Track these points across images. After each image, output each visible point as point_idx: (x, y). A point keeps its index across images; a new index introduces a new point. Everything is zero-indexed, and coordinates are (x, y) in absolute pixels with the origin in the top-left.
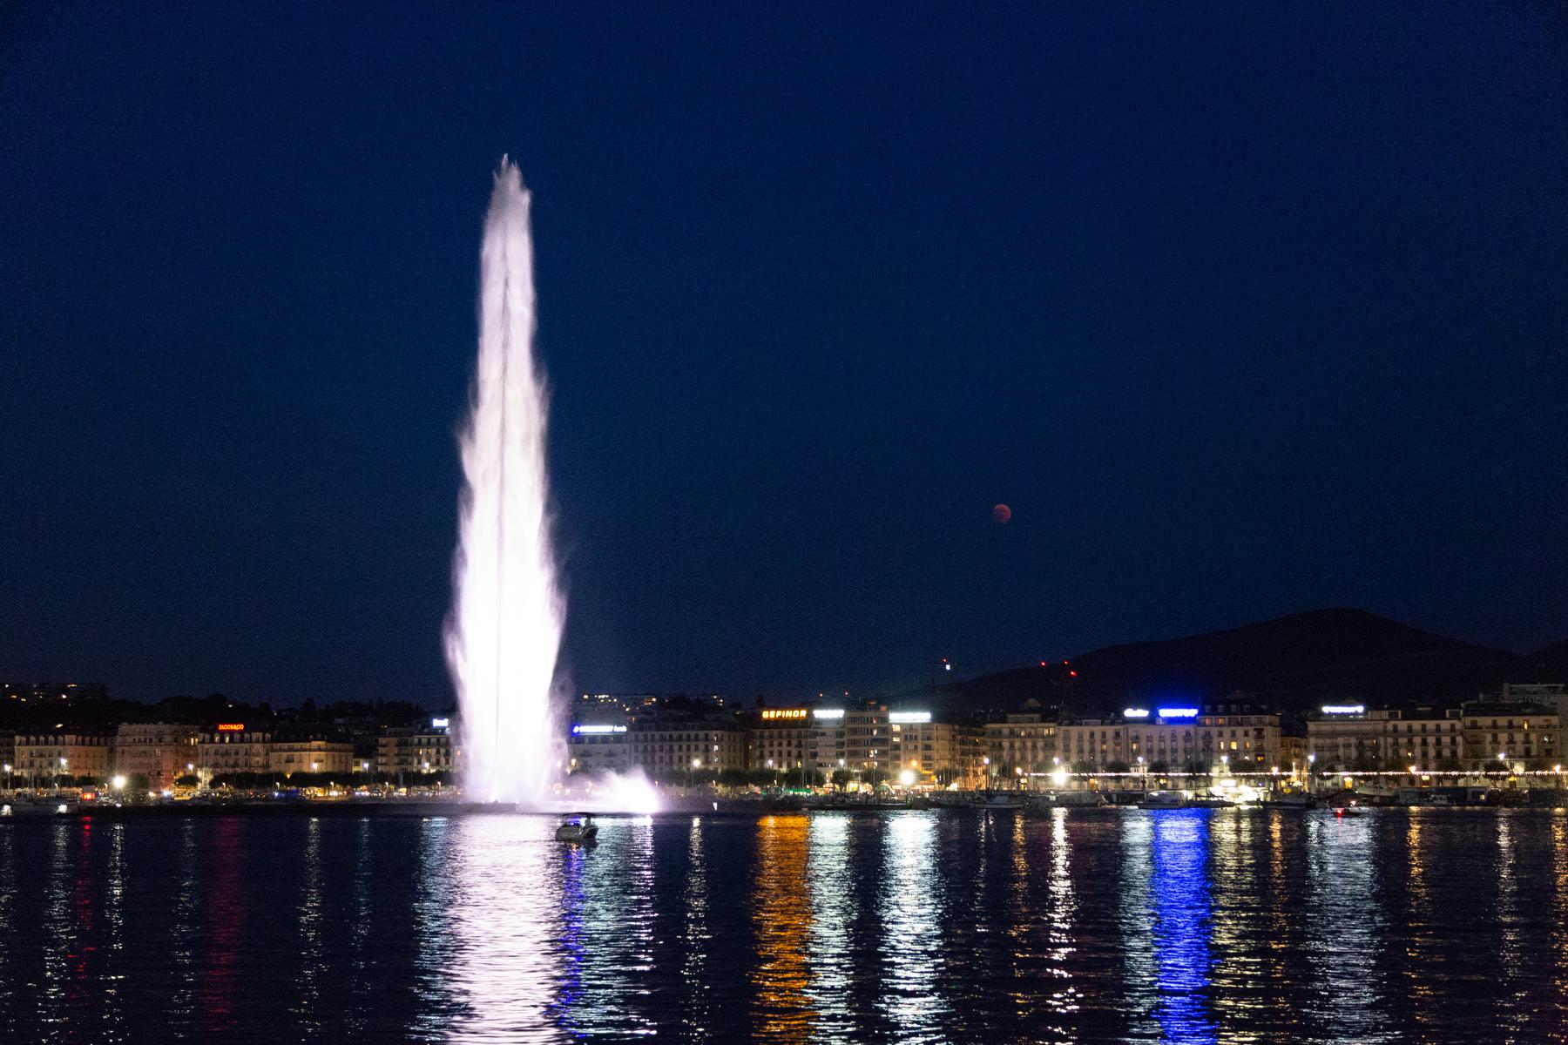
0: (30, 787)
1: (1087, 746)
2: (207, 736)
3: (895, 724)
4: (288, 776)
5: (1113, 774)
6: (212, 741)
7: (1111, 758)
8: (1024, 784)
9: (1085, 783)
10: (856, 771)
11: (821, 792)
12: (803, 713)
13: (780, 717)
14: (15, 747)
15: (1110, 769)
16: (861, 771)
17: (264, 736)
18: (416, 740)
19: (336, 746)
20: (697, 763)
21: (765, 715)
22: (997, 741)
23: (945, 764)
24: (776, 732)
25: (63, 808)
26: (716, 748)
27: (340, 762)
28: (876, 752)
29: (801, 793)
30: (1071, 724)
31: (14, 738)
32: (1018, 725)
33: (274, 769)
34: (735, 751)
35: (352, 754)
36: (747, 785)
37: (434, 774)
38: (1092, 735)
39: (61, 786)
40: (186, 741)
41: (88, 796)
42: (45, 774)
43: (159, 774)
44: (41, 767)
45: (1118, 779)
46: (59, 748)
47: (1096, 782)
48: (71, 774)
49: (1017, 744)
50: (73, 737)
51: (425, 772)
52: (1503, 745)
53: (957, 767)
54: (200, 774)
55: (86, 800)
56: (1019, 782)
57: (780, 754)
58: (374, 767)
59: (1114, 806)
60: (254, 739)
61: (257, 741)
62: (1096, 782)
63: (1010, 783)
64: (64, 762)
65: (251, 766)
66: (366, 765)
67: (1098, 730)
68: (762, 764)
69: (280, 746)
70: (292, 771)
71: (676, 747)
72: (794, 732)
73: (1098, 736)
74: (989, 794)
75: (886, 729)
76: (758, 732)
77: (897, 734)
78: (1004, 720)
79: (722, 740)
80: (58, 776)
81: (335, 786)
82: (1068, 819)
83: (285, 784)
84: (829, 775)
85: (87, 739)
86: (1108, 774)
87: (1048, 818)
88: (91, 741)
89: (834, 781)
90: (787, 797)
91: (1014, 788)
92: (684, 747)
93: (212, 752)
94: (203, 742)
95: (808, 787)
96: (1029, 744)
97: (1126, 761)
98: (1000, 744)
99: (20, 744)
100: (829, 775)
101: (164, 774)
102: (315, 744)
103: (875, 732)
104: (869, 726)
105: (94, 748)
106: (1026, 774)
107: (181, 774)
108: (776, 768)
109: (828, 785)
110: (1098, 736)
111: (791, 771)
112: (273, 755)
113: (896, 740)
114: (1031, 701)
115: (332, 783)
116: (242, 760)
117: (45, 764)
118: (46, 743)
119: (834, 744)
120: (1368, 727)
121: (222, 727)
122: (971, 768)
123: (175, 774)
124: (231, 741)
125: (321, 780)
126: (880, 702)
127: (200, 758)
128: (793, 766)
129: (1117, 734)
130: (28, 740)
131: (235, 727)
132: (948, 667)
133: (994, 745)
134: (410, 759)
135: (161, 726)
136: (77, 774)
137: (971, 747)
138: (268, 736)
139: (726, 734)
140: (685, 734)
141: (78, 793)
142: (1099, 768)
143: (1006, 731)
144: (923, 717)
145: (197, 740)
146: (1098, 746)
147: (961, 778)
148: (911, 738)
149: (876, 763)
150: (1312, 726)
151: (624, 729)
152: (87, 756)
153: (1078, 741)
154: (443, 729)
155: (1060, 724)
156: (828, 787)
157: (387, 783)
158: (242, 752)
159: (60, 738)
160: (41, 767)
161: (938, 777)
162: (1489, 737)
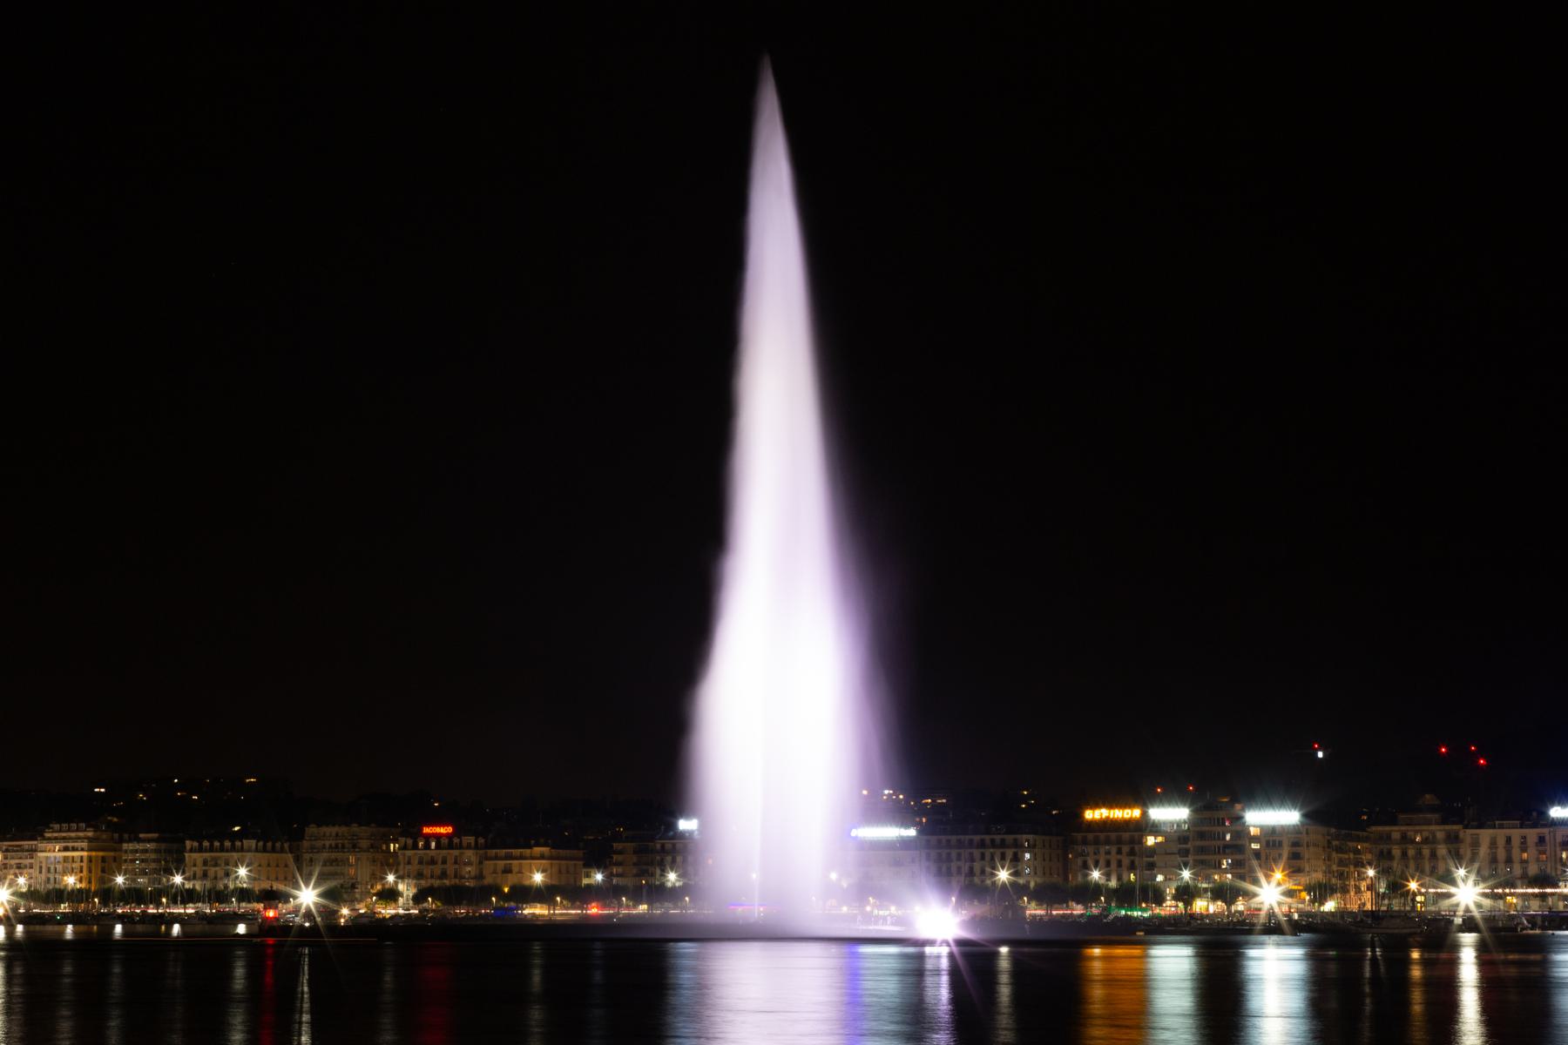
0: (204, 902)
1: (1501, 854)
2: (410, 842)
3: (1254, 826)
4: (506, 890)
5: (1536, 891)
6: (415, 847)
7: (1533, 870)
8: (1420, 902)
9: (1501, 902)
10: (1205, 885)
11: (1158, 911)
12: (1136, 813)
13: (1108, 818)
14: (186, 855)
15: (1531, 884)
16: (1210, 886)
17: (476, 842)
18: (658, 846)
19: (562, 852)
20: (1003, 875)
21: (1090, 815)
22: (1385, 847)
23: (1318, 876)
24: (1102, 836)
25: (241, 929)
26: (1027, 856)
27: (568, 872)
28: (1230, 861)
29: (1135, 914)
30: (1480, 826)
31: (184, 843)
32: (1410, 828)
33: (488, 880)
34: (1050, 860)
35: (581, 863)
36: (1067, 903)
37: (679, 887)
38: (1509, 840)
39: (239, 901)
40: (384, 847)
41: (271, 914)
42: (221, 886)
43: (353, 886)
44: (216, 878)
45: (1543, 896)
46: (236, 855)
47: (1515, 901)
48: (250, 886)
49: (1411, 852)
50: (253, 843)
51: (669, 885)
53: (1334, 881)
54: (401, 887)
55: (269, 918)
56: (1413, 900)
57: (1108, 864)
58: (609, 877)
59: (1538, 932)
60: (464, 844)
61: (469, 847)
62: (1515, 901)
63: (1402, 901)
64: (242, 872)
65: (462, 877)
66: (599, 877)
67: (1516, 834)
68: (1087, 875)
69: (496, 854)
70: (510, 883)
72: (1126, 836)
73: (1516, 842)
74: (1373, 915)
75: (1242, 833)
76: (1079, 836)
77: (1255, 839)
78: (1394, 822)
79: (1034, 846)
80: (236, 889)
81: (561, 902)
82: (1482, 948)
84: (1170, 891)
85: (269, 844)
86: (1530, 891)
87: (1455, 947)
88: (273, 847)
89: (1176, 898)
90: (1117, 918)
91: (1408, 908)
92: (988, 857)
93: (200, 862)
94: (404, 848)
95: (1144, 905)
96: (1426, 852)
97: (1554, 874)
98: (1389, 852)
99: (191, 851)
100: (1170, 891)
101: (359, 886)
102: (538, 850)
103: (1228, 837)
104: (1220, 829)
105: (260, 854)
106: (1423, 890)
107: (379, 887)
108: (1102, 881)
109: (1168, 903)
110: (1516, 842)
111: (1121, 886)
112: (489, 865)
113: (1255, 846)
114: (1428, 796)
115: (558, 899)
116: (450, 871)
117: (221, 873)
118: (222, 849)
119: (1176, 851)
121: (426, 830)
122: (1353, 883)
123: (372, 887)
124: (437, 847)
125: (543, 895)
126: (1235, 799)
127: (401, 867)
128: (1125, 878)
129: (1541, 840)
130: (201, 845)
131: (442, 830)
132: (1320, 755)
133: (1381, 852)
134: (651, 869)
135: (355, 828)
136: (257, 887)
137: (1352, 856)
138: (481, 841)
139: (1039, 838)
140: (987, 838)
141: (259, 911)
142: (1519, 883)
143: (1396, 836)
144: (1287, 817)
145: (397, 845)
146: (1516, 852)
147: (1339, 895)
148: (1274, 845)
149: (1229, 876)
151: (912, 832)
152: (269, 865)
153: (1490, 848)
154: (691, 833)
155: (1466, 827)
156: (1170, 907)
157: (624, 899)
158: (450, 861)
159: (238, 844)
160: (216, 878)
161: (1309, 894)
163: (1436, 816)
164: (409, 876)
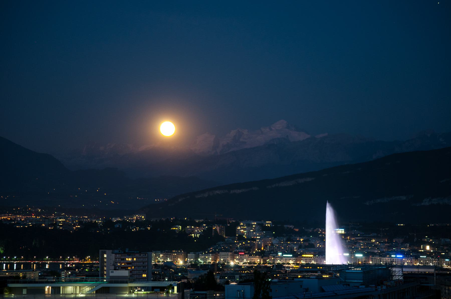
30: (384, 257)
49: (376, 260)
52: (445, 263)
71: (321, 259)
83: (430, 265)
99: (201, 255)
120: (427, 259)
121: (240, 253)
131: (242, 253)
135: (228, 253)
143: (374, 258)
150: (419, 259)
155: (382, 257)
162: (443, 261)
163: (379, 256)
164: (237, 260)
